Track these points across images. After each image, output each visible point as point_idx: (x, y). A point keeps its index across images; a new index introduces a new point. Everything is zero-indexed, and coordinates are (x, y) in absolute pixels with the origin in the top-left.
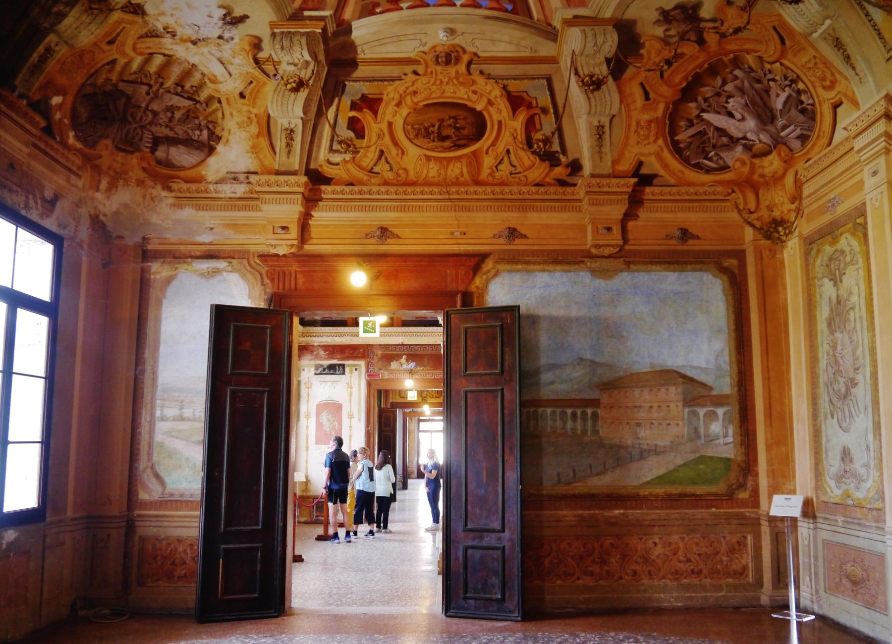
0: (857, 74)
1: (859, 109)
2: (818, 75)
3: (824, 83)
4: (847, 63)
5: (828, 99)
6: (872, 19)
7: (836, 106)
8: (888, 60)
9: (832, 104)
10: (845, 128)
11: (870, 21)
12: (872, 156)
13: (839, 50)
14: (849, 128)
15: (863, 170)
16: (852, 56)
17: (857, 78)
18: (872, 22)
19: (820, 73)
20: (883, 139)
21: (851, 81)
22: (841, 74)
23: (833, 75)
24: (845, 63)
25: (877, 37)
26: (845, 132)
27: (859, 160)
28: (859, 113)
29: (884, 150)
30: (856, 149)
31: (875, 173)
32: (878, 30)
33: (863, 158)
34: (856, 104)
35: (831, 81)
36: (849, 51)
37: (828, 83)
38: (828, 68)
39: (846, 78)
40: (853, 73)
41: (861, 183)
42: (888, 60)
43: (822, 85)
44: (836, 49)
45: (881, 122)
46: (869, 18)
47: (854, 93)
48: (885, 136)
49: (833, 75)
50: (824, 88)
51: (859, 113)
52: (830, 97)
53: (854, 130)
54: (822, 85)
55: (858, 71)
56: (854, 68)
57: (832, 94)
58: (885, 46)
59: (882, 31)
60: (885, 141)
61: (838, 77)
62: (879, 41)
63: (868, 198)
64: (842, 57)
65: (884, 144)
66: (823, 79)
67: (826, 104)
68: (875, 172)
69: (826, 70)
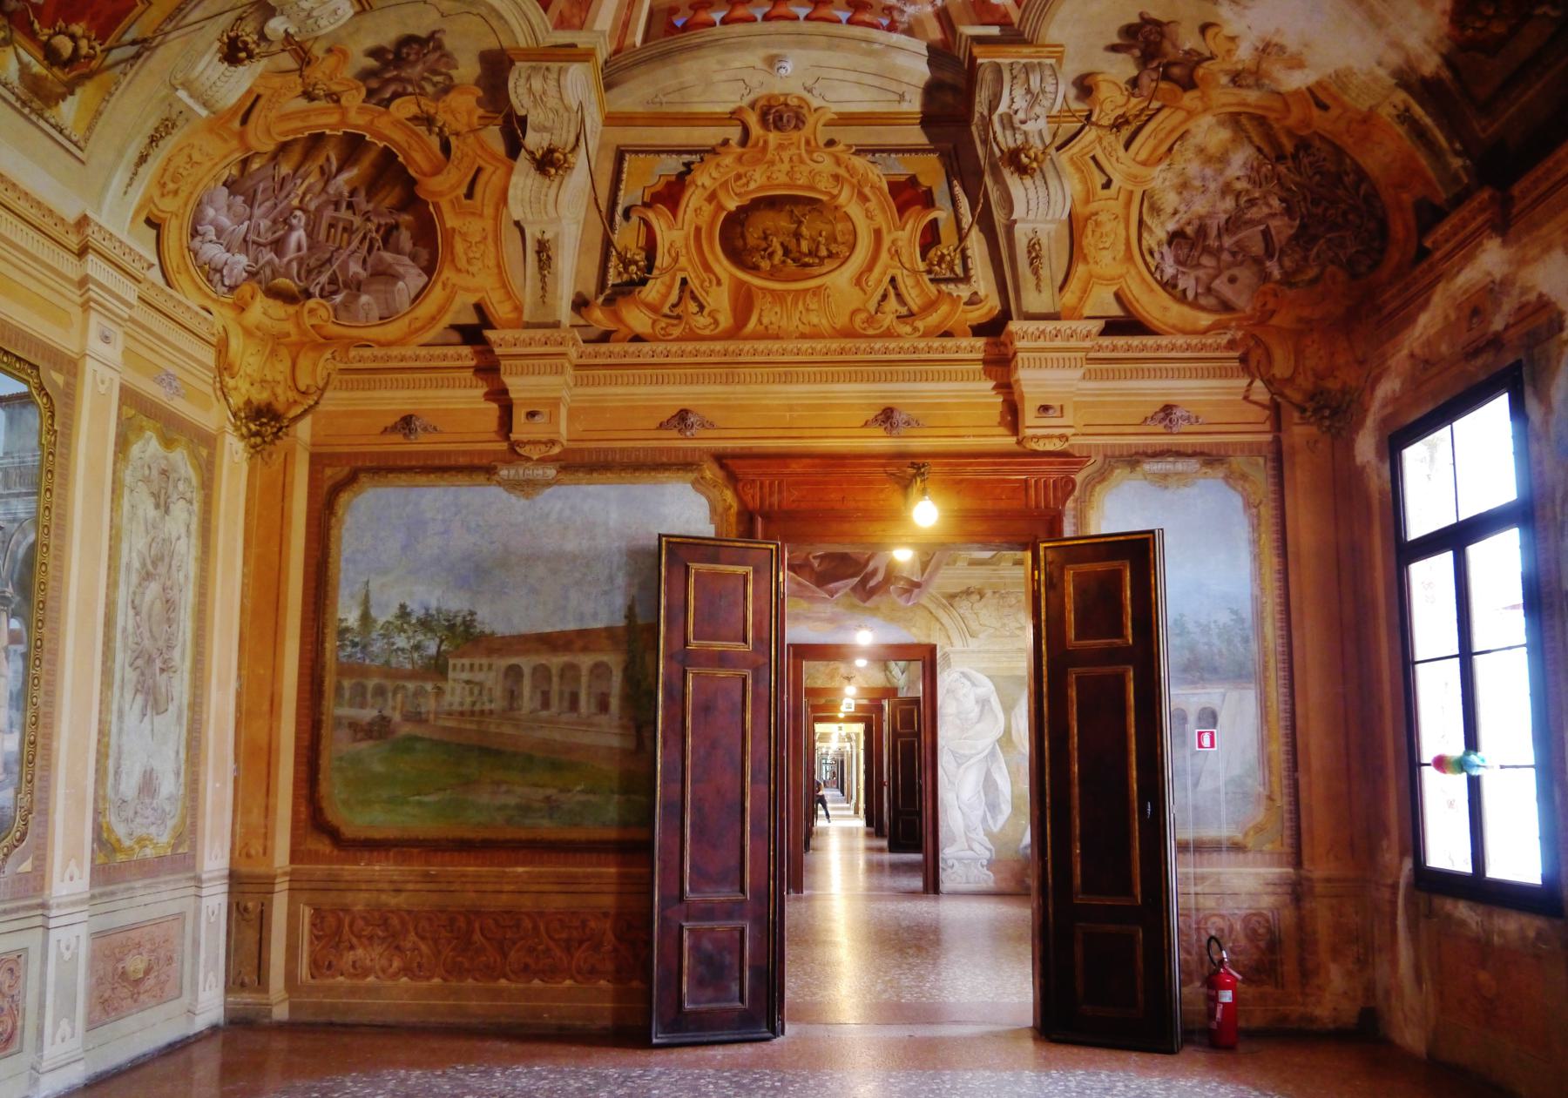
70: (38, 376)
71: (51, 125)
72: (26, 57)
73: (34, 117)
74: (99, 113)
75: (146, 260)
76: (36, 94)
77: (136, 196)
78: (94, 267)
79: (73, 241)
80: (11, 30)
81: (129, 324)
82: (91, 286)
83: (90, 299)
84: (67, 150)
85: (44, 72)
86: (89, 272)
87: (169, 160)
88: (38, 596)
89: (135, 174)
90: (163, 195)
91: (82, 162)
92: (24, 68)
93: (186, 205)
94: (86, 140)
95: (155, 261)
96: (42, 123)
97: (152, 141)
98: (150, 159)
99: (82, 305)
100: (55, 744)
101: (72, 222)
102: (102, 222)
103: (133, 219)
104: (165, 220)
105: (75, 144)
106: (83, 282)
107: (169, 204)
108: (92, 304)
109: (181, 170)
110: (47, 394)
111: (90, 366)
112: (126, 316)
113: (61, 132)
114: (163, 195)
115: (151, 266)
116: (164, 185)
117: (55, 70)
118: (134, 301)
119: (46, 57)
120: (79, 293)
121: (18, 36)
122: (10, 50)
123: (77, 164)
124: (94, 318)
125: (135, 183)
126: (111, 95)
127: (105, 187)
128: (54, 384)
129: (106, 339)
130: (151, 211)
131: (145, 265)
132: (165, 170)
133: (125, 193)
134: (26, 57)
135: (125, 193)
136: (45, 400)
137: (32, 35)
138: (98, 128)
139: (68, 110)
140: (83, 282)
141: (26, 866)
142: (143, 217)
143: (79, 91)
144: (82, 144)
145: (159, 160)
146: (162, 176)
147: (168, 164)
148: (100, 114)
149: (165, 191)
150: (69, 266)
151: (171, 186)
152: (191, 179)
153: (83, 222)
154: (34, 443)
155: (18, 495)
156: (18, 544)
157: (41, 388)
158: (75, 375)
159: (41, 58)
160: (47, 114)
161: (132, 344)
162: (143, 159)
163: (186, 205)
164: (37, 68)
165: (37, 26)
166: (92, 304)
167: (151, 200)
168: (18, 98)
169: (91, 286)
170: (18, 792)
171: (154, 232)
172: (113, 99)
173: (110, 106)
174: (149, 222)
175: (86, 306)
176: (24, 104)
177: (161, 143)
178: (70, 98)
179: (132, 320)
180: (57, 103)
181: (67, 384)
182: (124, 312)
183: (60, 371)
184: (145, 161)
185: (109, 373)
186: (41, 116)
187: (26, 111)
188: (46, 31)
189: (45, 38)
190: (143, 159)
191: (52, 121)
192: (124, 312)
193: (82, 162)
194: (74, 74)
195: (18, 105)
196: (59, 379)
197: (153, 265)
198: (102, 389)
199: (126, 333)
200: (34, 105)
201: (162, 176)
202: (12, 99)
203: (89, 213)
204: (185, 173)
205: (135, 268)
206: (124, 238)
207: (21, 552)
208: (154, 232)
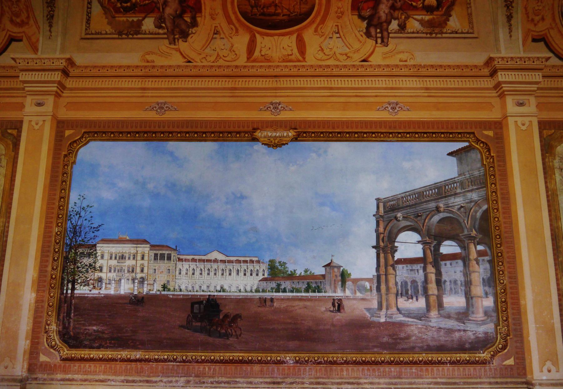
0: (50, 31)
1: (36, 54)
2: (14, 9)
3: (14, 18)
4: (48, 19)
5: (8, 30)
6: (91, 8)
7: (12, 39)
8: (82, 39)
9: (10, 35)
10: (13, 59)
11: (88, 8)
12: (37, 91)
13: (48, 7)
14: (18, 61)
15: (26, 97)
16: (55, 17)
17: (49, 33)
18: (89, 10)
19: (17, 9)
20: (56, 85)
21: (41, 33)
22: (36, 22)
23: (28, 17)
24: (45, 18)
25: (85, 20)
26: (13, 62)
27: (23, 89)
28: (34, 56)
29: (54, 93)
30: (20, 79)
31: (39, 104)
32: (90, 17)
33: (27, 89)
34: (35, 50)
35: (22, 21)
36: (56, 14)
37: (18, 20)
38: (27, 11)
39: (38, 28)
40: (48, 28)
41: (21, 106)
42: (82, 39)
43: (11, 18)
44: (46, 5)
45: (57, 73)
46: (89, 6)
47: (38, 40)
48: (58, 84)
49: (28, 17)
50: (12, 21)
51: (34, 56)
52: (10, 29)
53: (23, 65)
54: (11, 18)
55: (53, 29)
56: (51, 26)
57: (16, 30)
58: (86, 29)
59: (91, 19)
60: (57, 87)
61: (32, 22)
62: (84, 23)
63: (26, 120)
64: (46, 13)
65: (55, 89)
66: (17, 15)
67: (4, 33)
68: (39, 104)
69: (25, 12)
70: (475, 136)
71: (450, 33)
72: (419, 17)
73: (439, 36)
74: (470, 15)
75: (542, 58)
76: (434, 27)
77: (519, 34)
78: (501, 77)
79: (486, 71)
80: (406, 13)
81: (538, 91)
82: (503, 85)
83: (504, 91)
84: (465, 38)
85: (431, 17)
86: (500, 79)
87: (526, 8)
88: (495, 232)
89: (511, 25)
90: (535, 25)
91: (476, 38)
92: (421, 22)
93: (554, 19)
94: (472, 28)
95: (550, 55)
96: (444, 35)
97: (508, 7)
98: (514, 15)
99: (499, 96)
100: (522, 302)
101: (482, 64)
102: (502, 55)
103: (524, 45)
104: (546, 34)
105: (468, 33)
106: (498, 86)
107: (541, 27)
108: (506, 93)
109: (537, 8)
110: (483, 142)
111: (511, 120)
112: (536, 89)
113: (457, 33)
114: (535, 25)
115: (548, 59)
116: (533, 20)
117: (435, 13)
118: (541, 80)
119: (427, 12)
120: (495, 92)
121: (410, 13)
122: (411, 19)
123: (474, 40)
124: (509, 101)
125: (514, 29)
126: (470, 4)
127: (497, 40)
128: (487, 136)
129: (521, 104)
130: (532, 35)
131: (544, 60)
132: (527, 14)
133: (511, 36)
134: (419, 17)
135: (511, 36)
136: (482, 145)
137: (415, 8)
138: (474, 20)
139: (454, 23)
140: (498, 86)
141: (510, 362)
142: (530, 39)
143: (453, 13)
144: (471, 31)
145: (519, 11)
146: (528, 17)
147: (526, 10)
148: (471, 14)
149: (536, 22)
150: (489, 83)
151: (537, 18)
152: (547, 8)
153: (490, 60)
154: (479, 165)
155: (471, 191)
156: (476, 212)
157: (478, 141)
158: (501, 128)
159: (426, 13)
160: (445, 31)
161: (543, 100)
162: (509, 18)
163: (554, 19)
164: (427, 18)
165: (414, 4)
166: (506, 93)
167: (529, 30)
168: (427, 33)
169: (503, 85)
170: (497, 325)
171: (542, 43)
172: (472, 4)
173: (473, 8)
174: (534, 40)
175: (502, 96)
176: (431, 34)
177: (514, 5)
178: (451, 18)
179: (539, 89)
180: (446, 24)
181: (495, 134)
182: (534, 87)
183: (490, 129)
184: (512, 17)
185: (526, 120)
186: (442, 33)
187: (434, 35)
188: (419, 3)
189: (421, 5)
190: (509, 18)
191: (449, 31)
192: (534, 87)
193: (476, 38)
194: (444, 10)
195: (428, 36)
196: (490, 133)
197: (549, 58)
198: (524, 128)
199: (536, 97)
200: (436, 31)
201: (528, 17)
202: (424, 35)
203: (492, 55)
204: (540, 8)
205: (537, 65)
206: (522, 55)
207: (479, 215)
208: (542, 43)
